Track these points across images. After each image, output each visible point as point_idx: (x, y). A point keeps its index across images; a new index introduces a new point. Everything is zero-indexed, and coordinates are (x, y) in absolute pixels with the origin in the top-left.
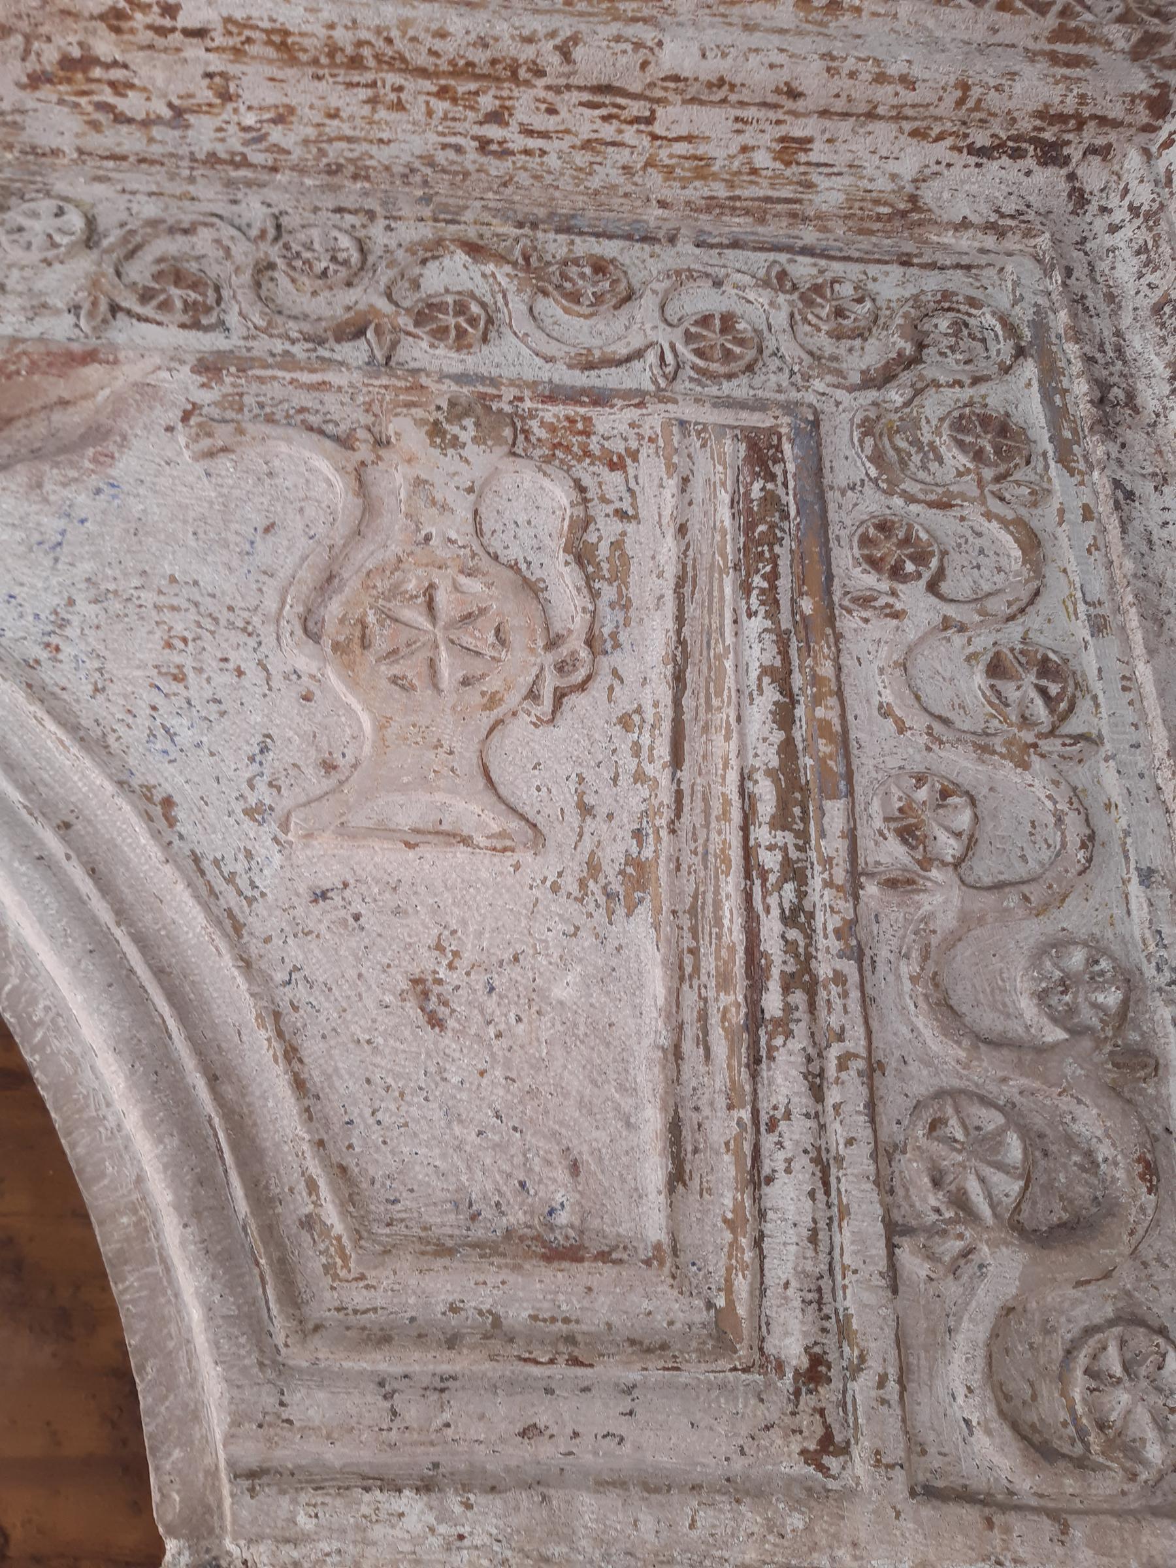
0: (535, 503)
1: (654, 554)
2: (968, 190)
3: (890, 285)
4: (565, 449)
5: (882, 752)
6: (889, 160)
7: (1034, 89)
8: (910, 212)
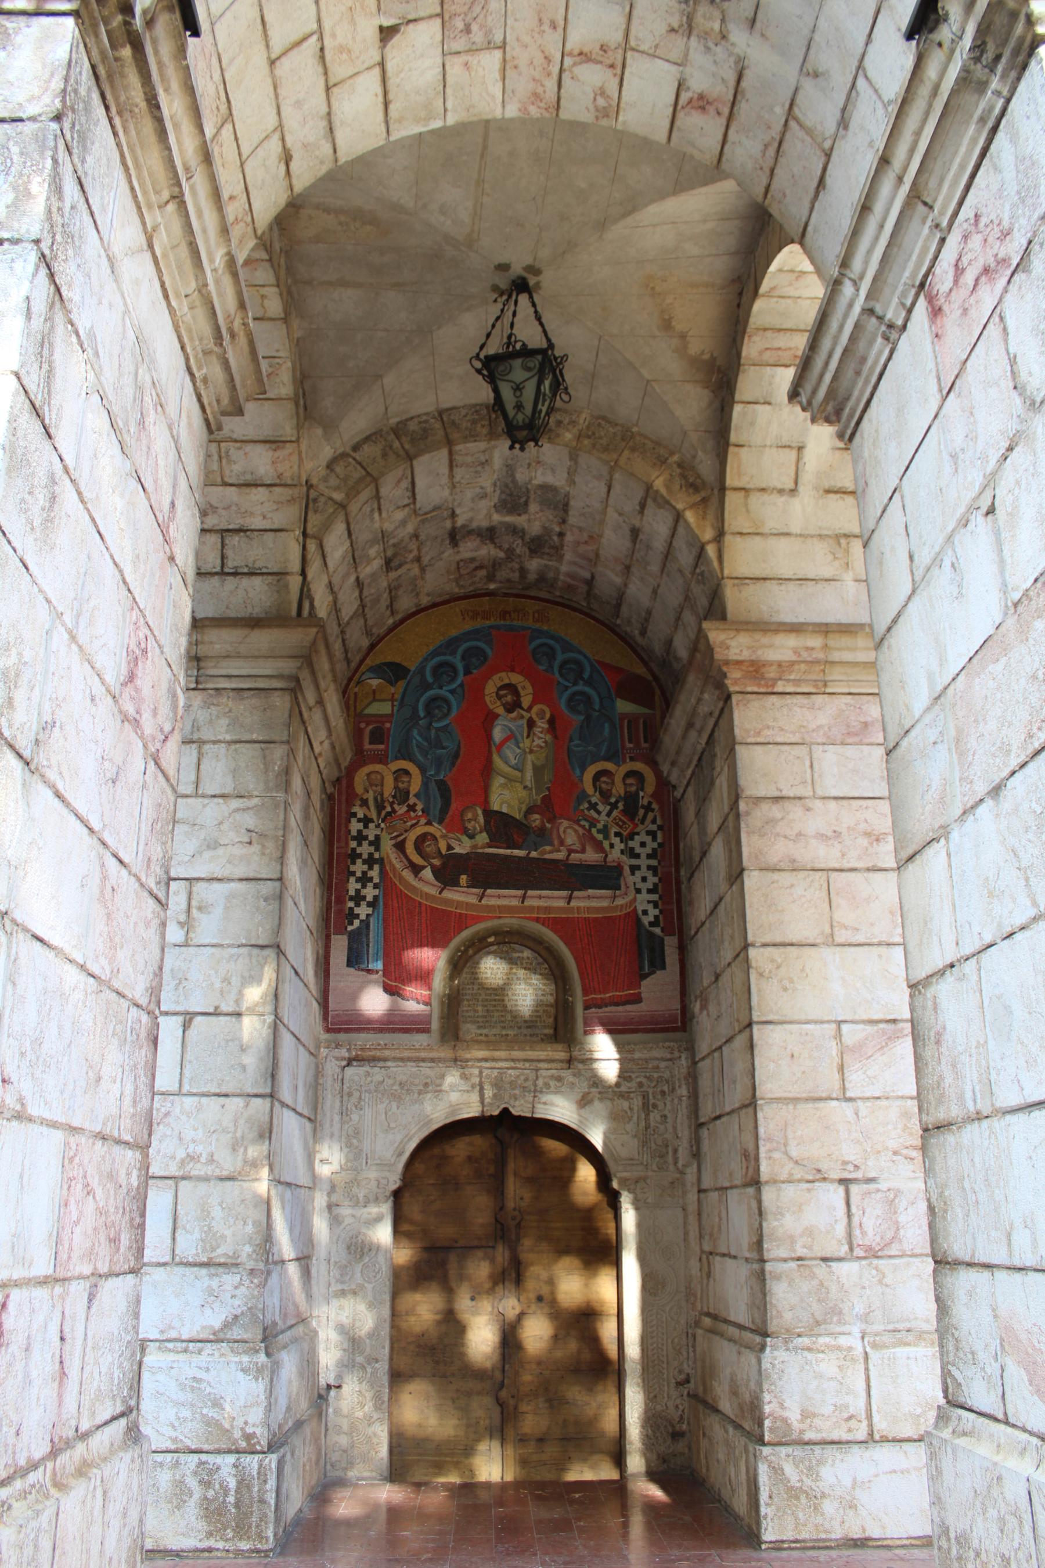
0: (626, 1104)
1: (636, 1108)
2: (663, 1065)
3: (656, 1075)
4: (628, 1098)
5: (652, 1124)
6: (655, 1063)
7: (669, 1056)
8: (658, 1067)
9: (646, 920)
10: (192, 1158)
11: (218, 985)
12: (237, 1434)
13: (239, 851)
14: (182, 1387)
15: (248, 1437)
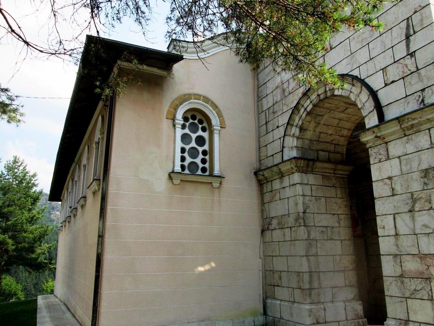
9: (356, 216)
10: (346, 267)
11: (345, 234)
12: (360, 316)
13: (344, 209)
14: (351, 308)
15: (361, 316)
